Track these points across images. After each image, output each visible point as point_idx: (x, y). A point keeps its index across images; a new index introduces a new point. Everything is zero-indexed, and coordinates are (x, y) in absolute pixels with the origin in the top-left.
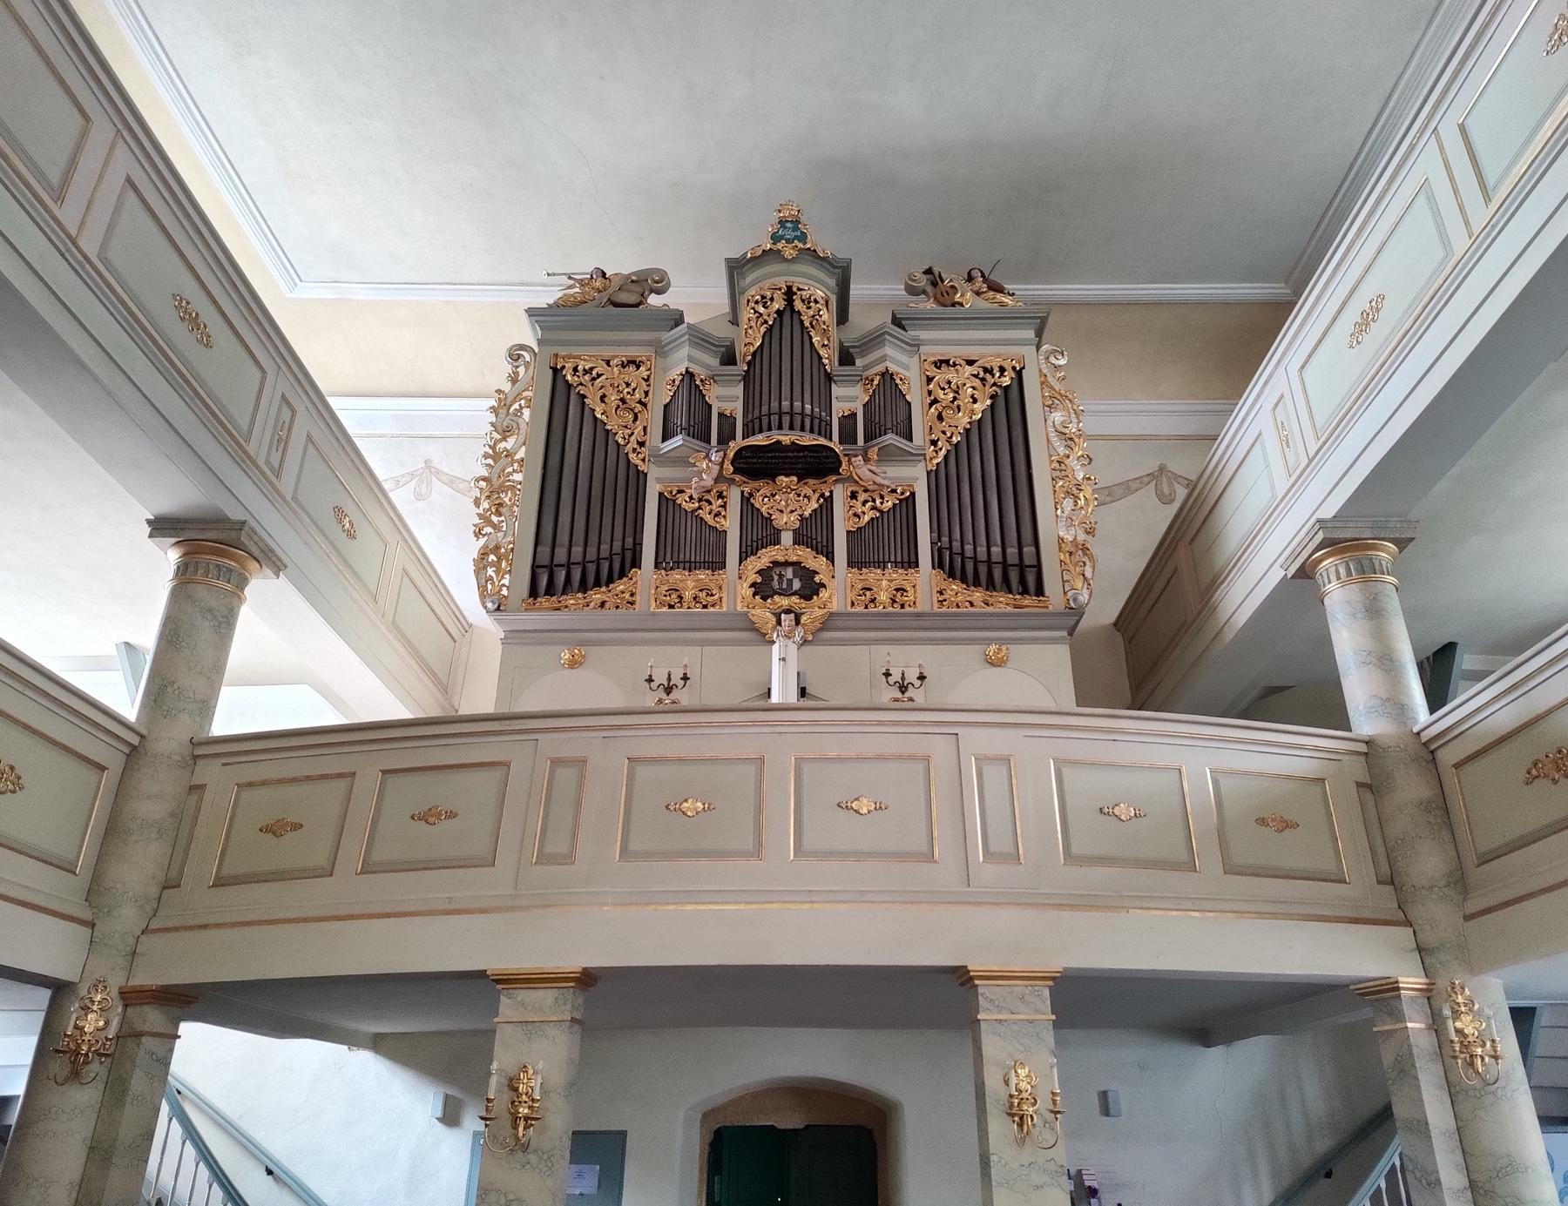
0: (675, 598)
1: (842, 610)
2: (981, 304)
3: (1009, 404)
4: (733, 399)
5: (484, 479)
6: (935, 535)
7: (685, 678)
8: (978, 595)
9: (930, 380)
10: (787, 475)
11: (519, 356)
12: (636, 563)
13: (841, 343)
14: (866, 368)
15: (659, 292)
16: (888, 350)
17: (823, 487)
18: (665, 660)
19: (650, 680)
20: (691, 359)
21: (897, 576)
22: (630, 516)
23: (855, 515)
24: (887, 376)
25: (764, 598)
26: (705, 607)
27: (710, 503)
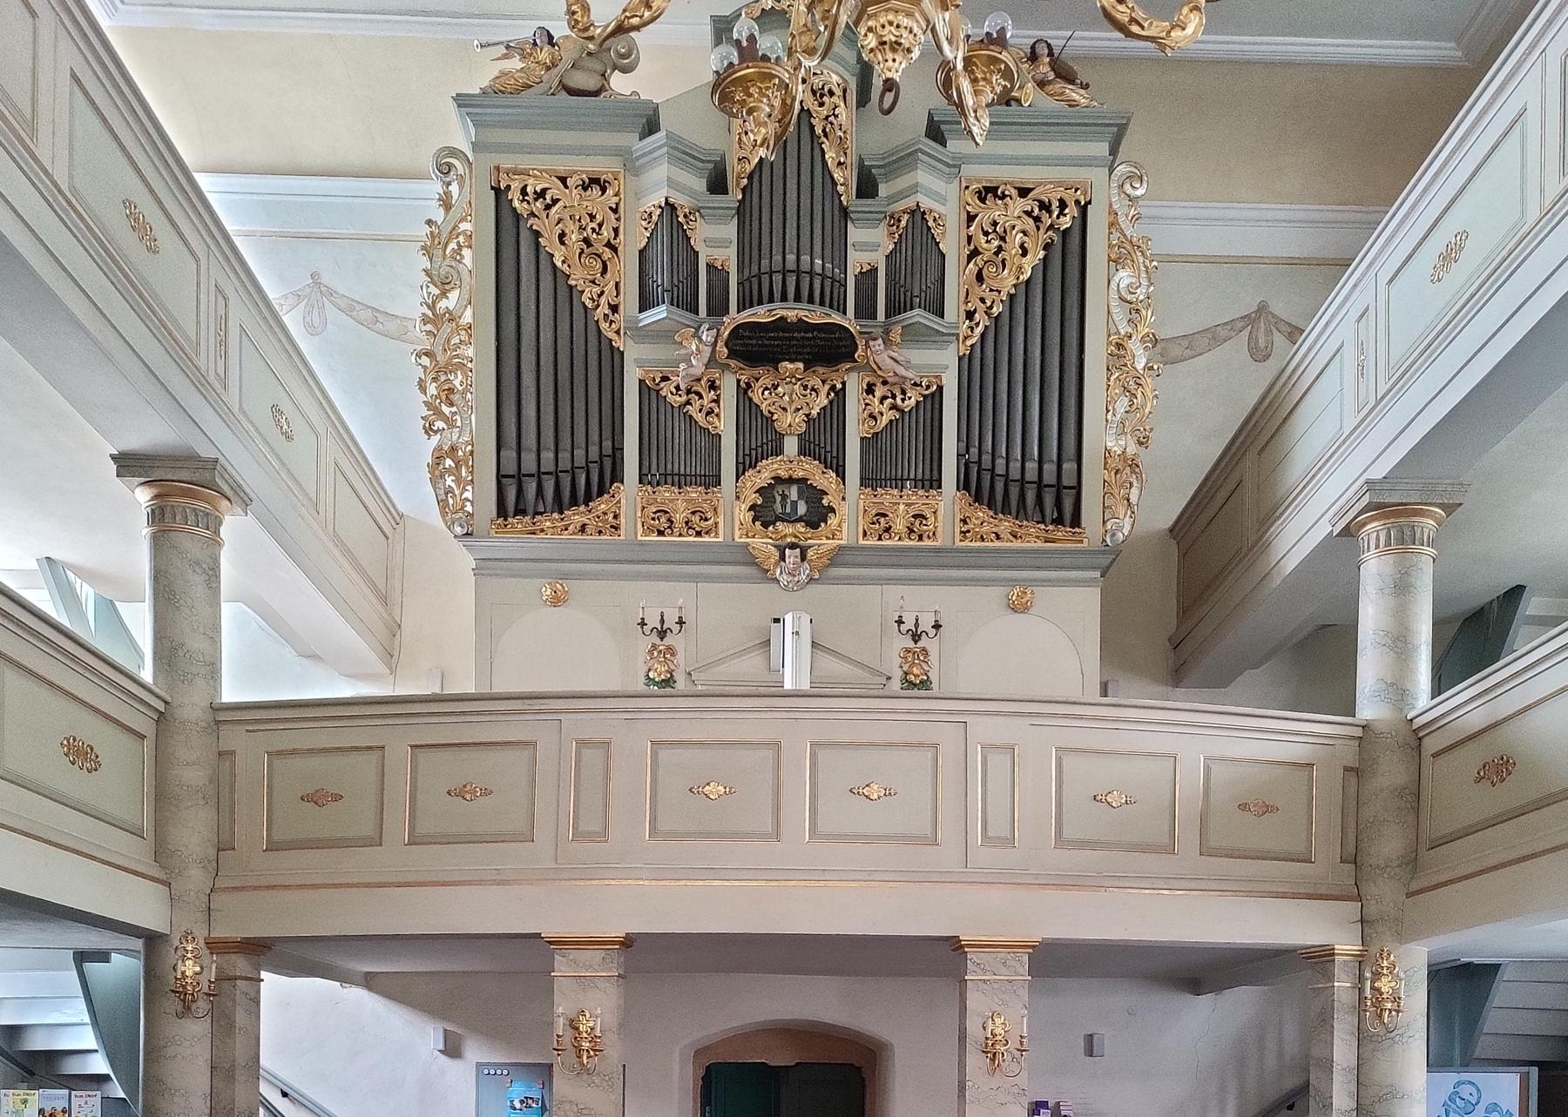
0: (663, 523)
1: (852, 542)
3: (1067, 257)
4: (724, 244)
6: (963, 445)
7: (681, 622)
8: (1006, 525)
9: (971, 218)
10: (792, 361)
11: (450, 166)
12: (617, 476)
13: (861, 160)
14: (893, 199)
15: (625, 70)
16: (922, 176)
17: (834, 376)
18: (659, 598)
20: (671, 183)
21: (916, 499)
23: (872, 416)
25: (765, 525)
26: (699, 534)
27: (701, 397)
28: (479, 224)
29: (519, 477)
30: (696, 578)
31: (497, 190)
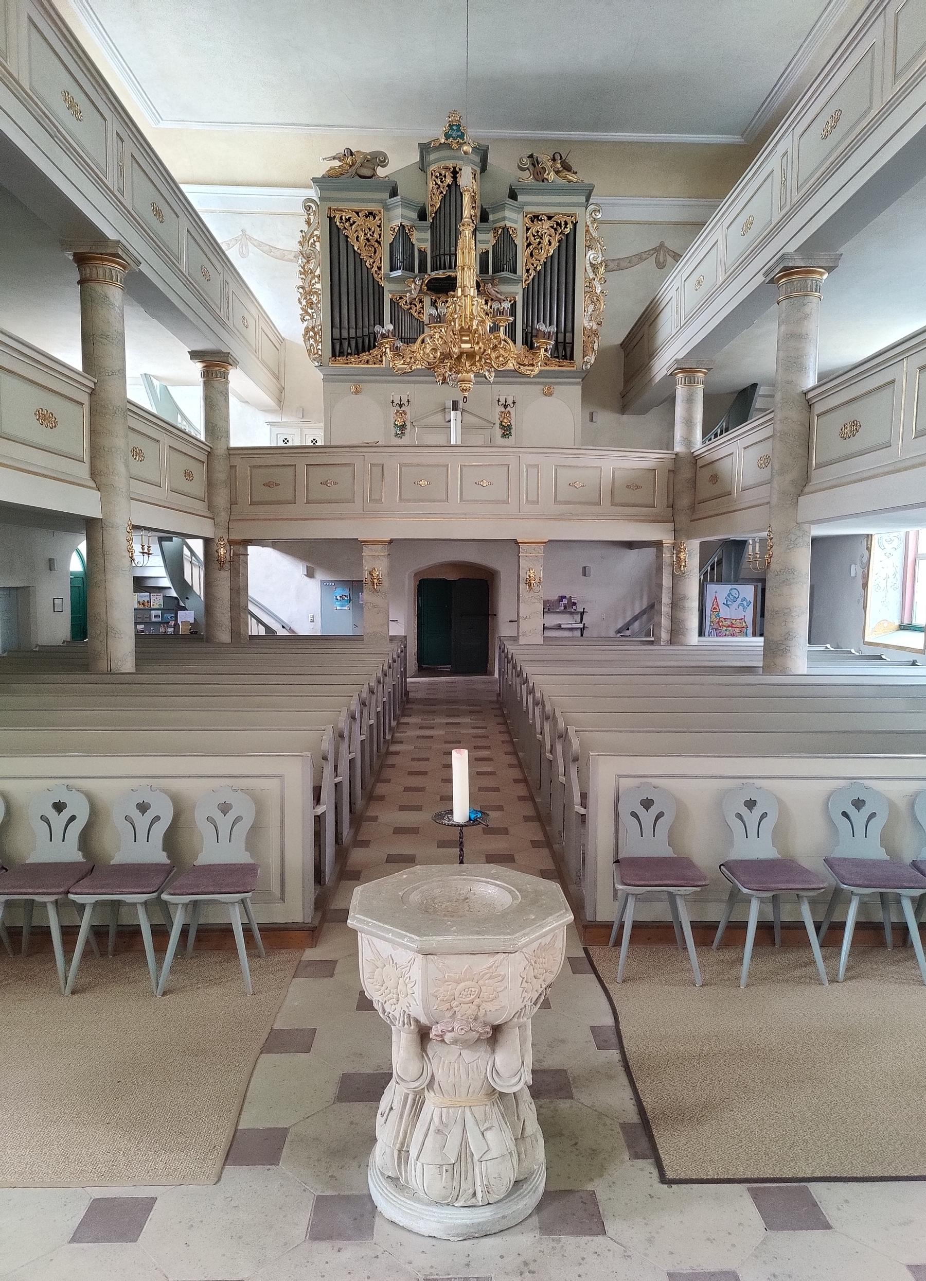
2: (560, 181)
3: (568, 246)
5: (303, 288)
9: (528, 229)
11: (310, 207)
14: (495, 222)
15: (382, 167)
16: (508, 213)
18: (399, 391)
19: (393, 402)
20: (403, 217)
22: (377, 311)
24: (505, 229)
28: (321, 232)
29: (341, 340)
30: (415, 382)
31: (330, 218)
